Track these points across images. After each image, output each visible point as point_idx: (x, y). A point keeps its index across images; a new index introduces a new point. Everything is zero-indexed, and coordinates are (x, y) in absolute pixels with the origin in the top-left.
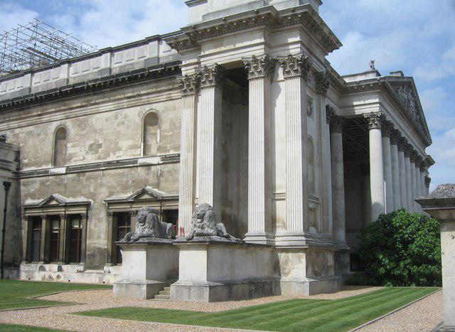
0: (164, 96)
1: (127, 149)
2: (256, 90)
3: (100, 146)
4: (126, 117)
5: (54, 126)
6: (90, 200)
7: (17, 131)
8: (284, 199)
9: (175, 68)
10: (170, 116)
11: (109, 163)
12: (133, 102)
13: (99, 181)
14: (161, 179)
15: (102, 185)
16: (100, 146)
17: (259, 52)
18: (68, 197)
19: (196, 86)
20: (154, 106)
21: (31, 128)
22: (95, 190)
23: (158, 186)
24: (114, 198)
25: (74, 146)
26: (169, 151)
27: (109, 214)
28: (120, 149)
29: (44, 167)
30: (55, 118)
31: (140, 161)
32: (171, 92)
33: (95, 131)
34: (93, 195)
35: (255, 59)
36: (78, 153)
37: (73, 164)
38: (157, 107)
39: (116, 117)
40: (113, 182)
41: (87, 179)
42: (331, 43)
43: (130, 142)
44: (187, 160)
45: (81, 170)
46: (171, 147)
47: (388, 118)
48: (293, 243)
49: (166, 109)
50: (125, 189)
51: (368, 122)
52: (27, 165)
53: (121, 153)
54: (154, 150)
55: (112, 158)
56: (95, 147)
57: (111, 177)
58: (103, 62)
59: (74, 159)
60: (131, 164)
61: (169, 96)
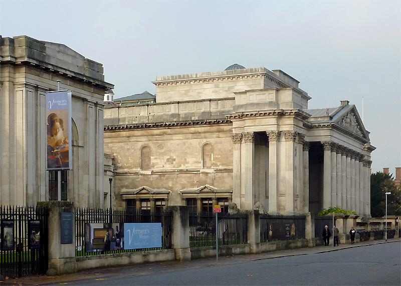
0: (215, 135)
1: (193, 162)
3: (174, 160)
4: (191, 144)
5: (140, 145)
6: (170, 191)
7: (110, 145)
10: (219, 147)
11: (181, 171)
12: (195, 136)
13: (175, 180)
14: (215, 181)
15: (177, 183)
16: (174, 160)
17: (274, 128)
18: (154, 188)
19: (239, 138)
20: (208, 140)
21: (122, 144)
22: (173, 185)
23: (213, 185)
24: (185, 190)
25: (156, 159)
27: (183, 199)
28: (188, 163)
29: (134, 170)
30: (140, 139)
31: (202, 171)
33: (170, 151)
34: (171, 188)
35: (272, 132)
36: (159, 163)
37: (155, 170)
38: (211, 140)
39: (184, 143)
40: (184, 181)
41: (167, 179)
42: (306, 98)
43: (194, 159)
45: (163, 174)
47: (336, 141)
49: (216, 143)
50: (193, 185)
51: (324, 146)
52: (121, 168)
53: (188, 165)
54: (208, 164)
55: (183, 167)
56: (170, 160)
57: (184, 179)
58: (173, 109)
59: (157, 166)
60: (196, 172)
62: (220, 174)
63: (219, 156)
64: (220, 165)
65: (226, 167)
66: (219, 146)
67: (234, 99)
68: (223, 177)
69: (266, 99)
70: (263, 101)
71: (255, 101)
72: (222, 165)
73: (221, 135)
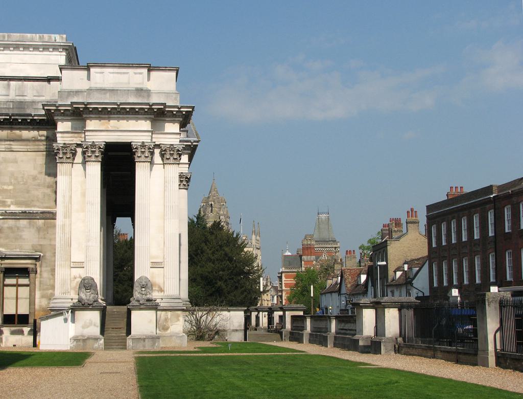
2: (141, 172)
8: (163, 268)
9: (22, 119)
10: (10, 169)
17: (146, 138)
26: (9, 206)
32: (11, 143)
35: (143, 145)
44: (64, 226)
46: (11, 202)
48: (172, 305)
61: (9, 146)
62: (11, 223)
63: (11, 187)
64: (12, 203)
65: (24, 209)
66: (11, 168)
67: (58, 79)
68: (18, 228)
69: (129, 83)
70: (125, 87)
71: (107, 85)
72: (17, 204)
73: (16, 146)
